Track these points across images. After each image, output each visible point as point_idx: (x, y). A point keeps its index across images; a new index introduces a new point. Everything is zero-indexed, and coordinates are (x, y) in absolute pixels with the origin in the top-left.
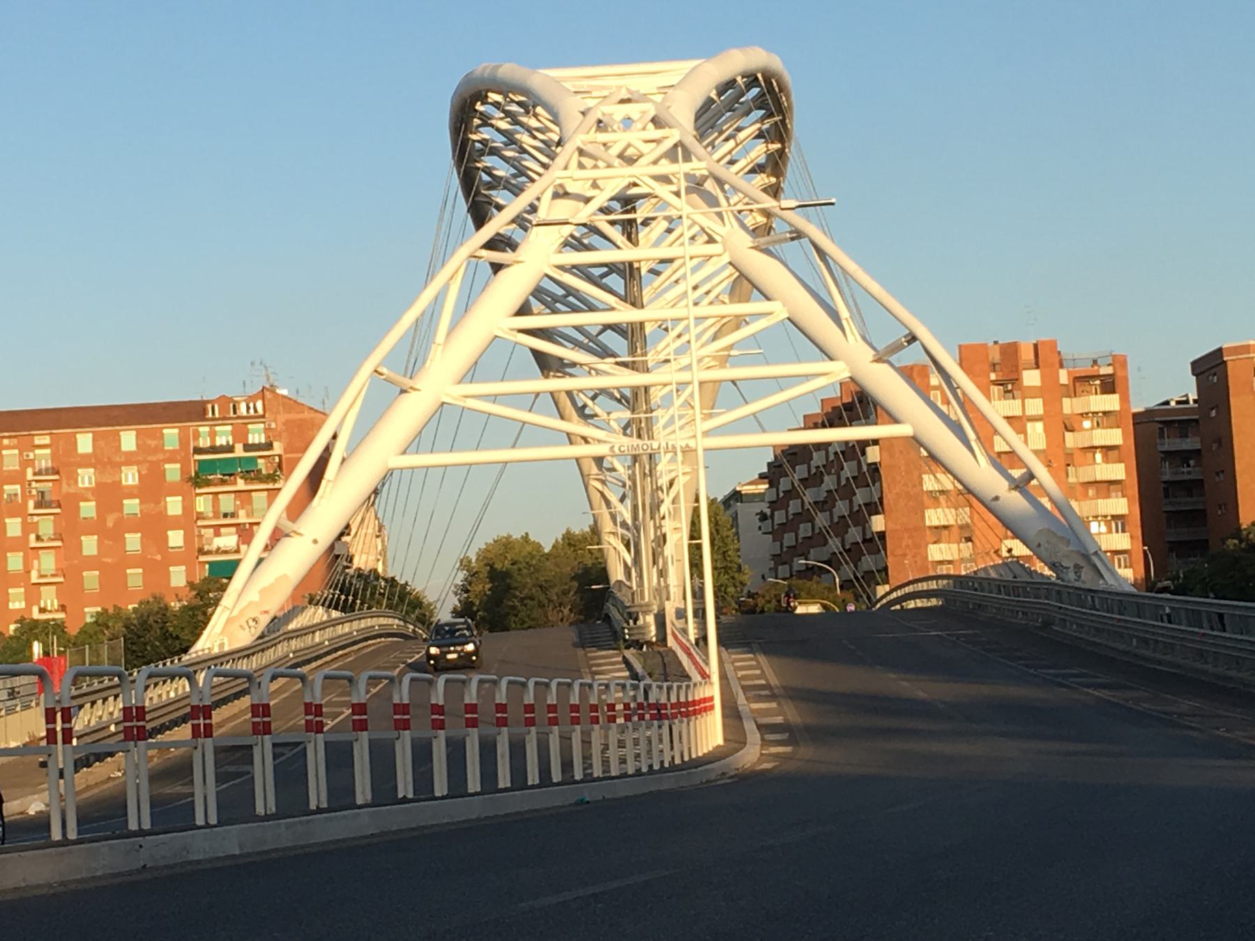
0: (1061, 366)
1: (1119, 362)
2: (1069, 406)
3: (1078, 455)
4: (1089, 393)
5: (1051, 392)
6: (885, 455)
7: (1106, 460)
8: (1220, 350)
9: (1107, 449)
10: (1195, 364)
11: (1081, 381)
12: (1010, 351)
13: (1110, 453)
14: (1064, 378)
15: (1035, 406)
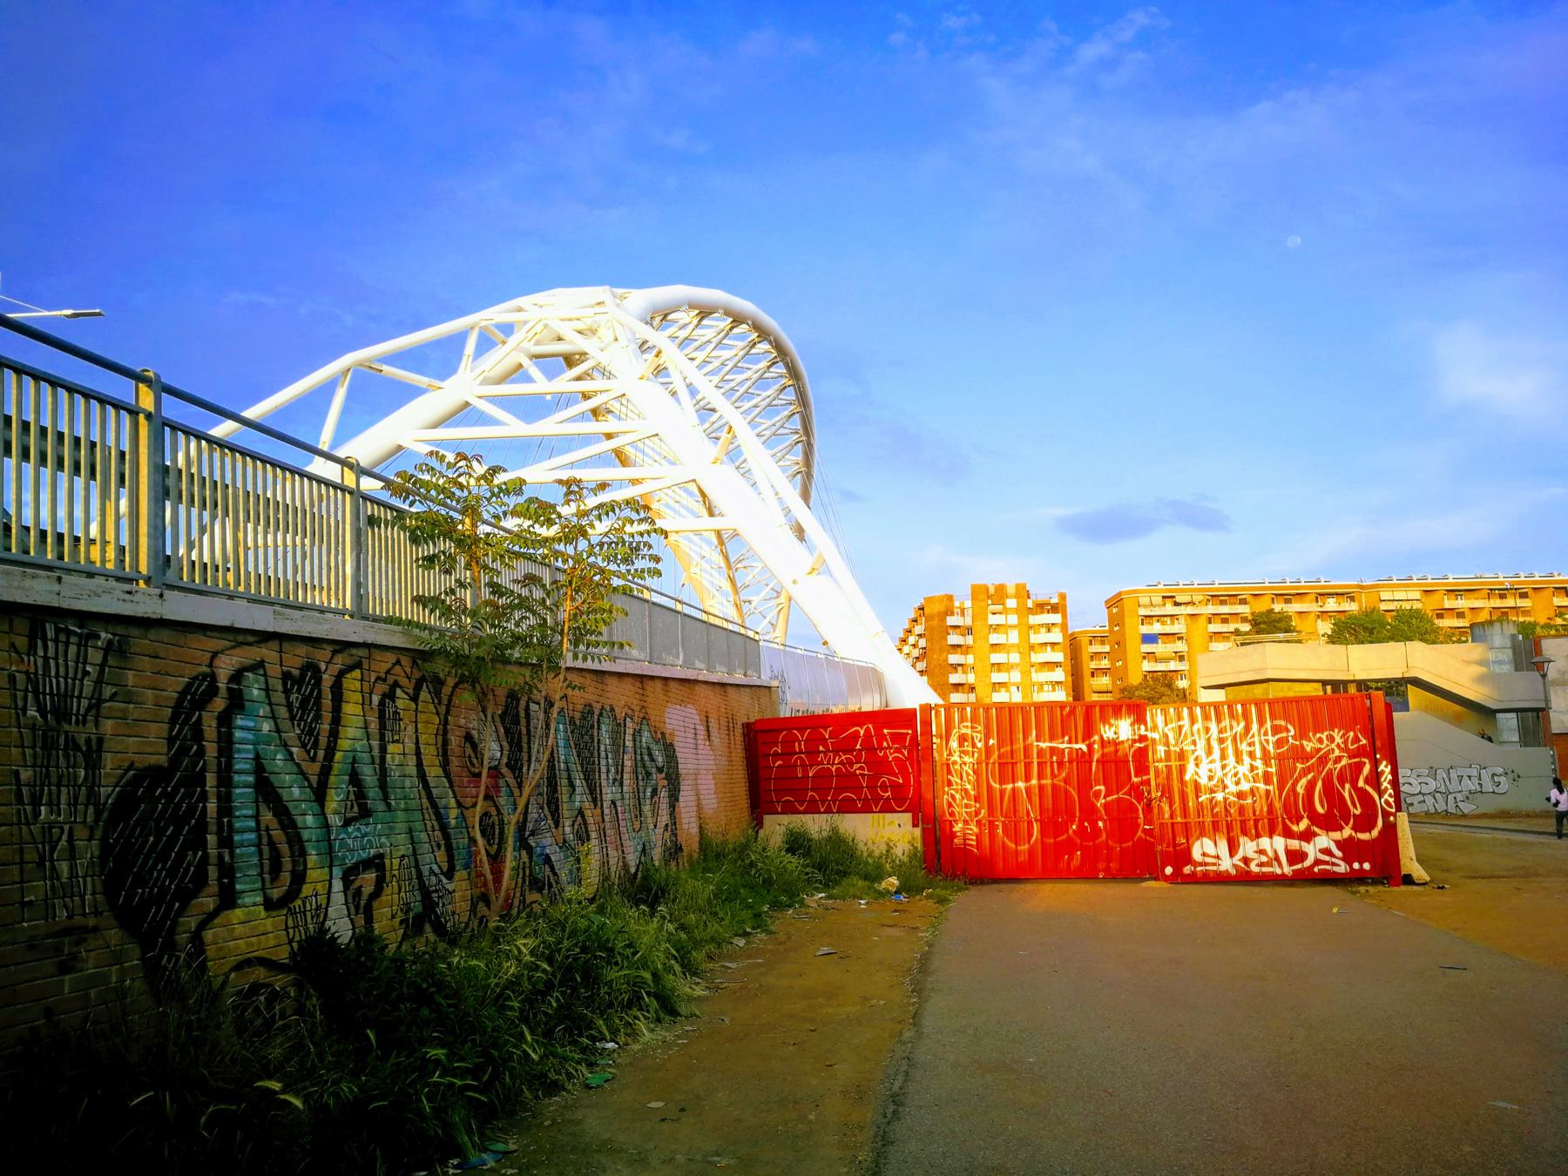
0: (1029, 597)
1: (1063, 597)
2: (1035, 619)
3: (1037, 648)
4: (1042, 613)
5: (1024, 611)
6: (929, 644)
7: (1053, 650)
8: (1120, 594)
9: (1053, 644)
10: (1107, 602)
11: (1041, 607)
12: (1001, 589)
13: (1056, 647)
14: (1030, 604)
15: (1013, 619)
